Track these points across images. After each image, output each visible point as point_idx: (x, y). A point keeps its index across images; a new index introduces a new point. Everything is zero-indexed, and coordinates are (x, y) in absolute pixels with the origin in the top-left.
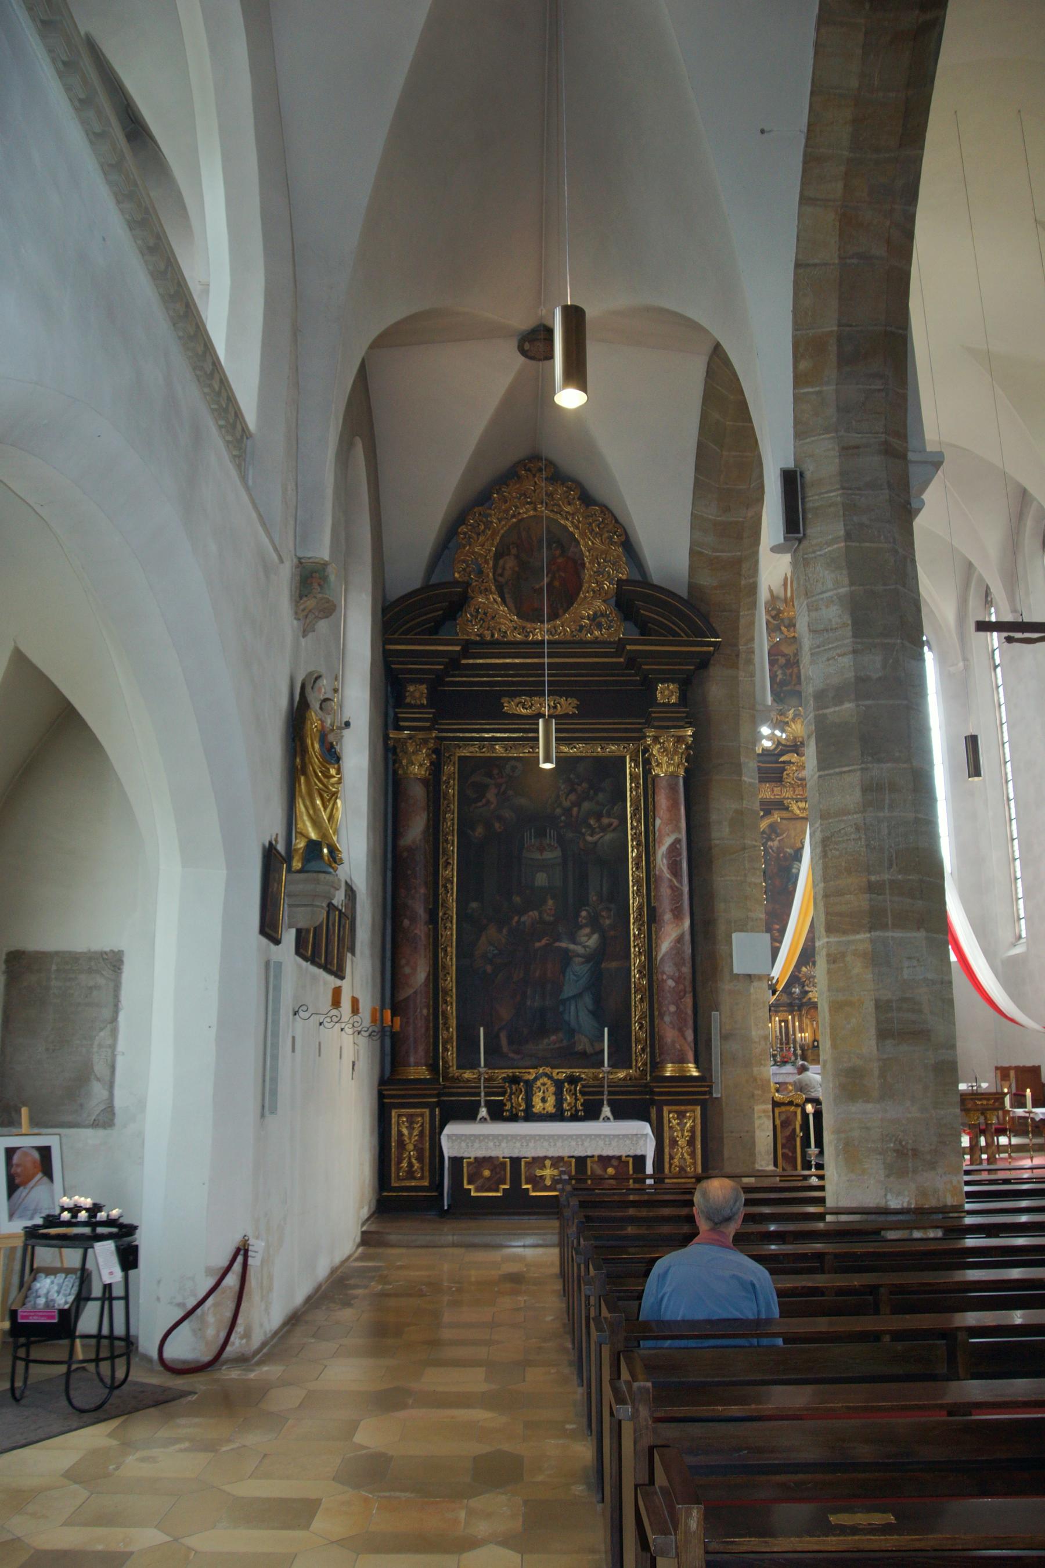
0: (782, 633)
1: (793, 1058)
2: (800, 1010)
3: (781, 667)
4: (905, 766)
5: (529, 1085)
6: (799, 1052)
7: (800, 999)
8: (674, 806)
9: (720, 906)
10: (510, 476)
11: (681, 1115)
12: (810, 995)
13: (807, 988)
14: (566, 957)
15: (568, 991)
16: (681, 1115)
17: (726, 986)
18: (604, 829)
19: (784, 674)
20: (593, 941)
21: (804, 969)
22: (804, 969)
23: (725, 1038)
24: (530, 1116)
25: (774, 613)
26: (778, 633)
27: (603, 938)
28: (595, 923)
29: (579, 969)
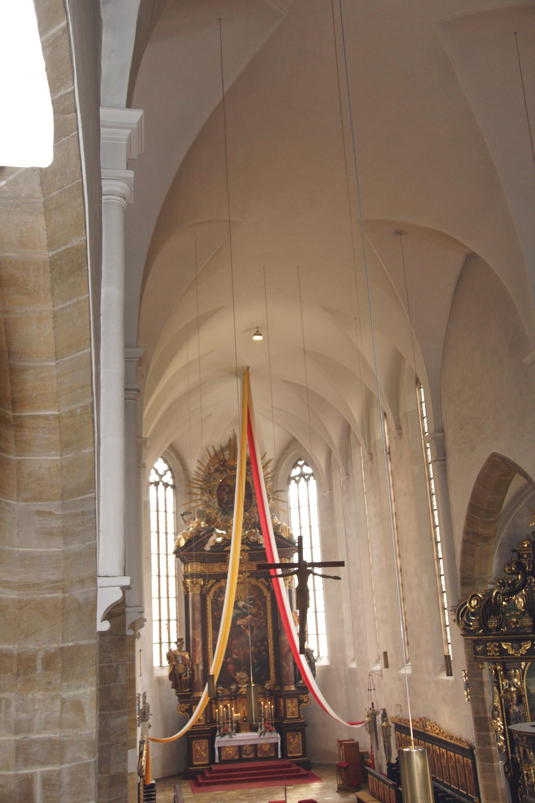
0: (227, 473)
1: (230, 731)
2: (236, 699)
3: (227, 493)
4: (106, 775)
6: (234, 725)
7: (236, 692)
12: (241, 690)
13: (240, 686)
19: (228, 497)
21: (238, 674)
22: (238, 674)
25: (221, 463)
26: (225, 473)
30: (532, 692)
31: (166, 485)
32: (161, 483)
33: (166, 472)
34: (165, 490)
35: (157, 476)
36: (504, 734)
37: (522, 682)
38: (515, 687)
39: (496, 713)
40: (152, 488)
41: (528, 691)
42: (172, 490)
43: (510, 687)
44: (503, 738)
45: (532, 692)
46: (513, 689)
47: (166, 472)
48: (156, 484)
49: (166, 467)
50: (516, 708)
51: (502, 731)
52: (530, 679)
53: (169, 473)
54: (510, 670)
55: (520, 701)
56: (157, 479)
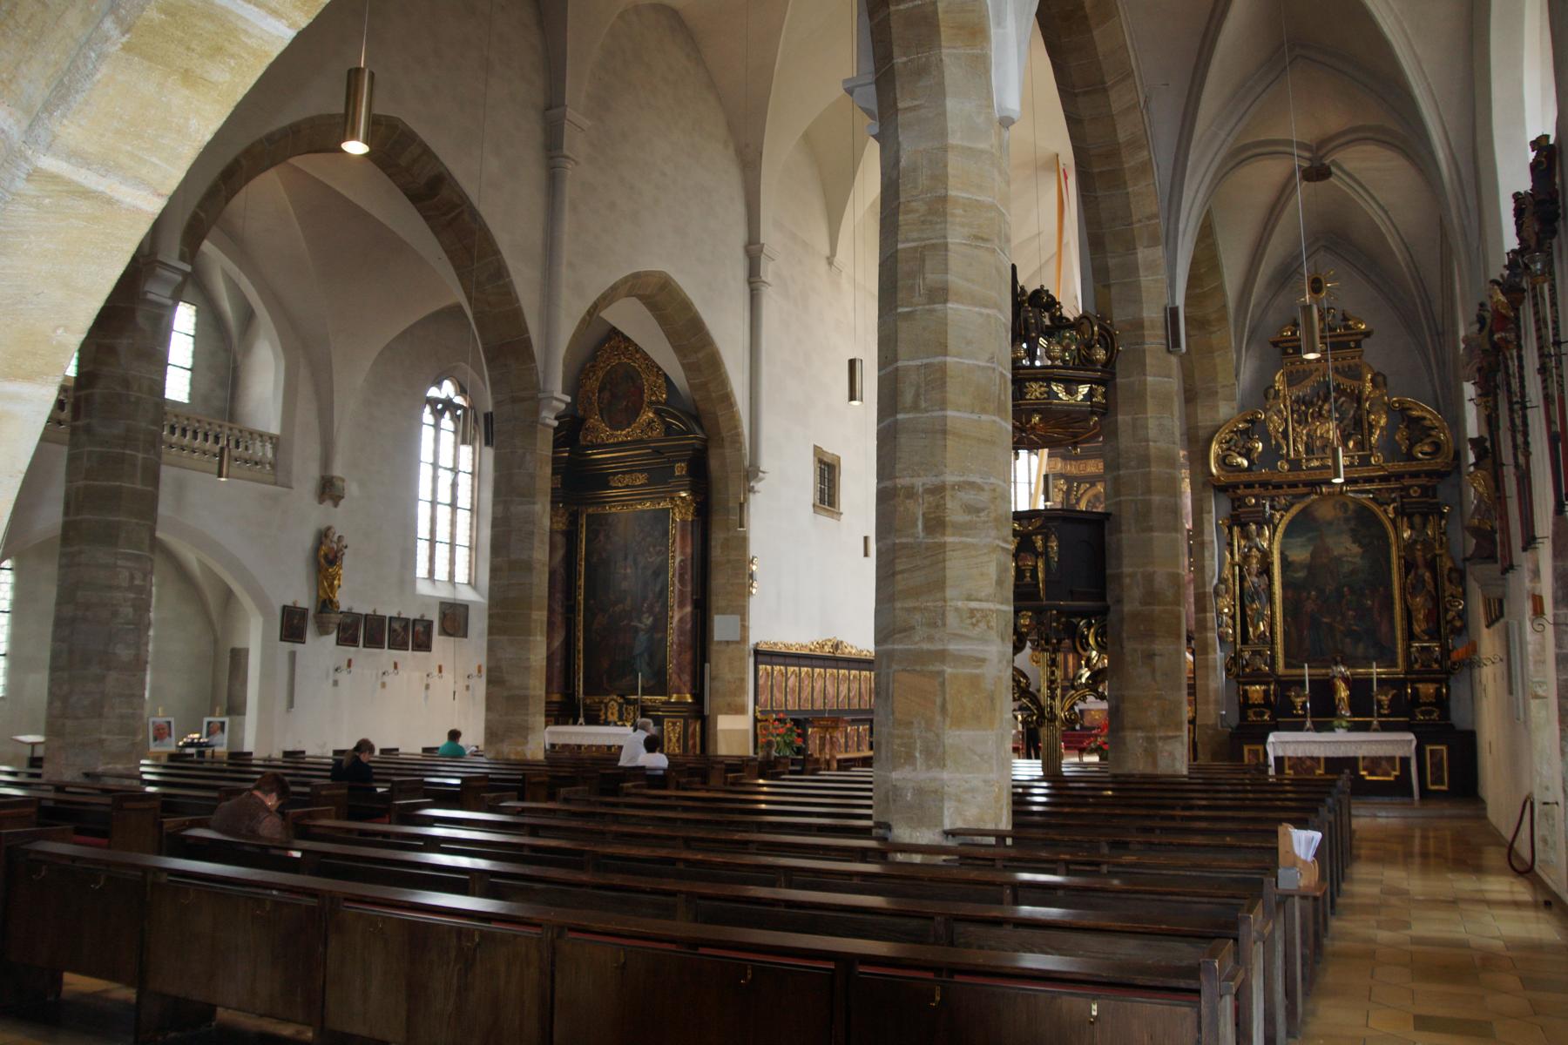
5: (606, 705)
8: (683, 538)
9: (714, 598)
10: (600, 346)
11: (674, 724)
14: (636, 630)
15: (637, 652)
16: (674, 724)
17: (714, 648)
18: (658, 553)
20: (649, 621)
23: (712, 679)
24: (606, 723)
27: (655, 620)
28: (650, 610)
29: (642, 637)
36: (1233, 617)
37: (1270, 544)
46: (1254, 552)
55: (1266, 570)
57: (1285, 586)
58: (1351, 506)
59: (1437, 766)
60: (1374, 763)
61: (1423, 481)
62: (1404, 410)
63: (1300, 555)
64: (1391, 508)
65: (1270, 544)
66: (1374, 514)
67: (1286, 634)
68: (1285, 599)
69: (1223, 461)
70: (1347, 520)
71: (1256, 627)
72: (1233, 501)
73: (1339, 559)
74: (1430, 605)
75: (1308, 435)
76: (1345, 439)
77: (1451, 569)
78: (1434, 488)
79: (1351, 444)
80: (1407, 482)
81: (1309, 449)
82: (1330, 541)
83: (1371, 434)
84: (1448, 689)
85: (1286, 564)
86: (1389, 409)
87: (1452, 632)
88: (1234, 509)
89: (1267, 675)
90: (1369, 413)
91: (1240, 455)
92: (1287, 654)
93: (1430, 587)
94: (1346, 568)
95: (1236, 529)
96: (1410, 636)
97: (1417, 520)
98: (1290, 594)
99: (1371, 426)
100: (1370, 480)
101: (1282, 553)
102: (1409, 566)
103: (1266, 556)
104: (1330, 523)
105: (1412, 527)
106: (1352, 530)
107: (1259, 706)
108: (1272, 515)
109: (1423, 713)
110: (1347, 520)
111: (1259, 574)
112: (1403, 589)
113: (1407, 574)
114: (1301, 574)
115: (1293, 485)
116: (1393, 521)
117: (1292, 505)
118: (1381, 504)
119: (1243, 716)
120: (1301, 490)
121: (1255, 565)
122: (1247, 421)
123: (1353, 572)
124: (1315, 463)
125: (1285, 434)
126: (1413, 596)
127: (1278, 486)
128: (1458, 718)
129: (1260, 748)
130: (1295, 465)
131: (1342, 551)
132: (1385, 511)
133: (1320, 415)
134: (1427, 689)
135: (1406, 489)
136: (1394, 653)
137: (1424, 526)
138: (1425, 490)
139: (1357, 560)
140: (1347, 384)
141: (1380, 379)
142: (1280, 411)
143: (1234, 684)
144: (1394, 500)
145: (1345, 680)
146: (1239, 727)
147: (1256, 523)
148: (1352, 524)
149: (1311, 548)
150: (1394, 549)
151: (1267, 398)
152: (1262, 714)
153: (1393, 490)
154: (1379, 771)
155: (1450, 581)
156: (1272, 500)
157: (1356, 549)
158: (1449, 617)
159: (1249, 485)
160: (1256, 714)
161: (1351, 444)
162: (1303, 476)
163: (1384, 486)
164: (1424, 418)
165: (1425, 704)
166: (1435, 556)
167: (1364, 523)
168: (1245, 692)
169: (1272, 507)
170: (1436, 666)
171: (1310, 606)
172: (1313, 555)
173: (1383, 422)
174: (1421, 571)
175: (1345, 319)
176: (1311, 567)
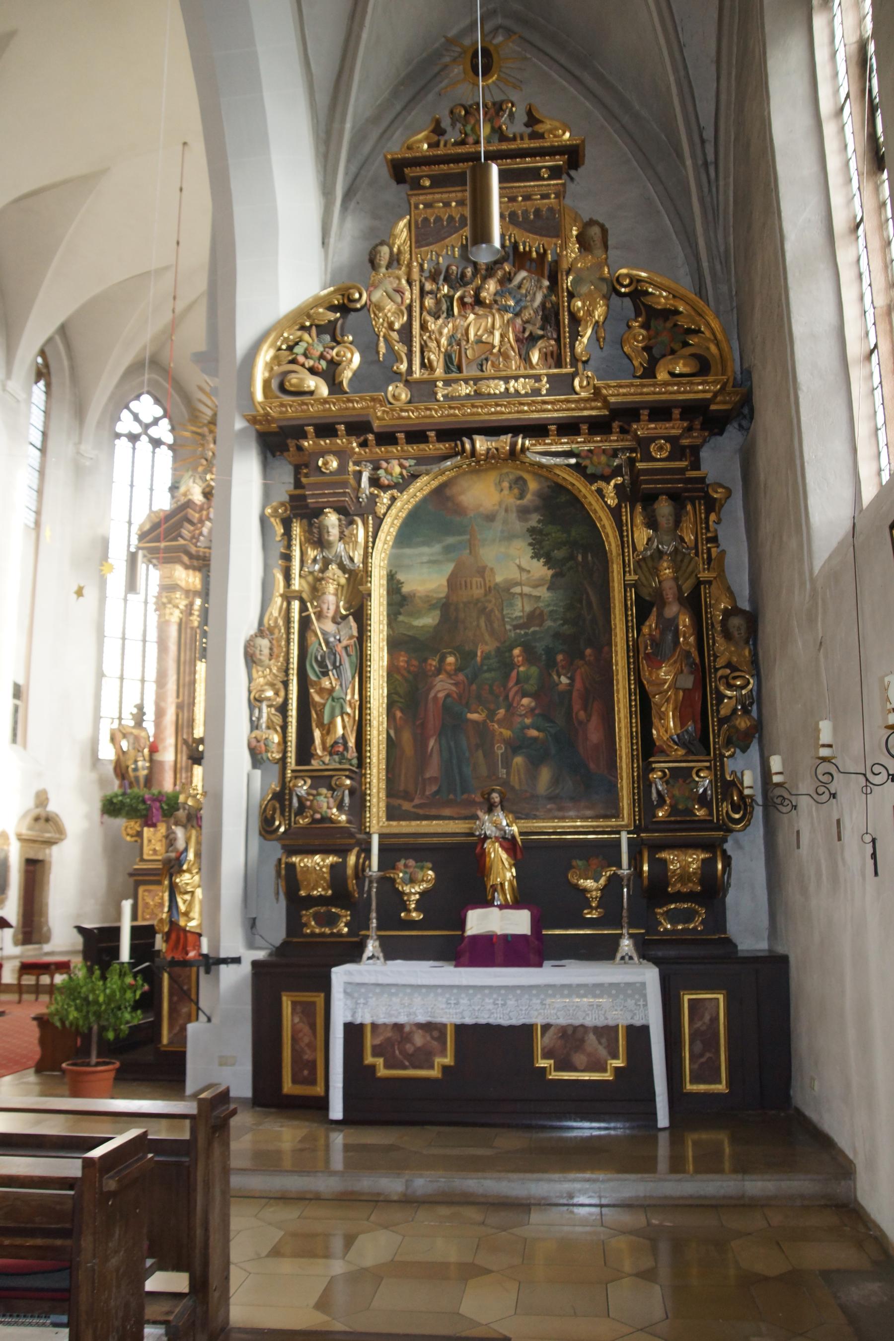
30: (405, 589)
31: (156, 443)
32: (144, 438)
33: (156, 421)
34: (154, 453)
35: (137, 424)
37: (367, 556)
38: (342, 567)
39: (264, 643)
40: (123, 444)
41: (394, 586)
42: (170, 453)
43: (324, 569)
44: (278, 720)
45: (405, 589)
47: (156, 421)
48: (133, 438)
49: (159, 411)
50: (330, 627)
51: (280, 700)
52: (407, 551)
53: (165, 424)
54: (318, 512)
55: (359, 613)
56: (136, 429)
57: (394, 644)
58: (533, 485)
59: (706, 1039)
60: (570, 1040)
61: (674, 428)
62: (638, 295)
63: (427, 580)
64: (610, 489)
65: (367, 556)
66: (575, 501)
67: (392, 744)
68: (392, 672)
69: (282, 386)
70: (524, 512)
71: (328, 729)
72: (297, 469)
73: (504, 592)
74: (688, 681)
75: (451, 337)
76: (527, 342)
77: (727, 614)
78: (695, 450)
79: (535, 357)
80: (643, 429)
81: (452, 364)
82: (489, 554)
83: (575, 335)
84: (727, 861)
85: (398, 600)
86: (612, 289)
87: (729, 743)
88: (298, 484)
89: (343, 831)
90: (571, 295)
91: (312, 371)
92: (392, 791)
93: (688, 640)
94: (519, 610)
95: (297, 530)
96: (647, 748)
97: (664, 508)
98: (402, 661)
99: (575, 320)
100: (568, 428)
101: (391, 577)
102: (644, 607)
103: (356, 582)
104: (490, 518)
105: (652, 523)
106: (532, 531)
107: (321, 900)
108: (373, 498)
109: (673, 917)
110: (524, 512)
111: (339, 619)
112: (634, 650)
113: (642, 618)
114: (429, 620)
115: (416, 436)
116: (616, 513)
117: (414, 477)
118: (592, 478)
119: (294, 924)
120: (434, 448)
121: (332, 599)
122: (332, 308)
123: (534, 617)
124: (464, 390)
125: (406, 334)
126: (656, 658)
127: (387, 438)
128: (746, 921)
129: (320, 999)
130: (423, 391)
131: (514, 574)
132: (600, 491)
133: (478, 301)
134: (685, 863)
135: (643, 444)
136: (613, 790)
137: (677, 523)
138: (678, 452)
139: (543, 592)
140: (531, 243)
141: (595, 231)
142: (399, 291)
143: (276, 850)
144: (617, 471)
145: (509, 844)
146: (285, 944)
147: (341, 510)
148: (534, 520)
149: (449, 568)
150: (616, 569)
151: (373, 263)
152: (332, 920)
153: (615, 453)
154: (579, 1059)
155: (727, 635)
156: (377, 468)
157: (539, 569)
158: (724, 711)
159: (326, 430)
160: (321, 920)
161: (535, 357)
162: (438, 414)
163: (598, 442)
164: (677, 312)
165: (679, 897)
166: (699, 583)
167: (558, 519)
168: (291, 867)
169: (374, 482)
170: (701, 813)
171: (442, 687)
172: (453, 582)
173: (599, 313)
174: (672, 610)
175: (532, 120)
176: (448, 609)
